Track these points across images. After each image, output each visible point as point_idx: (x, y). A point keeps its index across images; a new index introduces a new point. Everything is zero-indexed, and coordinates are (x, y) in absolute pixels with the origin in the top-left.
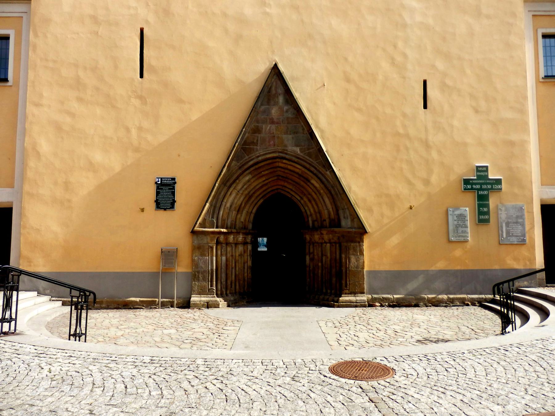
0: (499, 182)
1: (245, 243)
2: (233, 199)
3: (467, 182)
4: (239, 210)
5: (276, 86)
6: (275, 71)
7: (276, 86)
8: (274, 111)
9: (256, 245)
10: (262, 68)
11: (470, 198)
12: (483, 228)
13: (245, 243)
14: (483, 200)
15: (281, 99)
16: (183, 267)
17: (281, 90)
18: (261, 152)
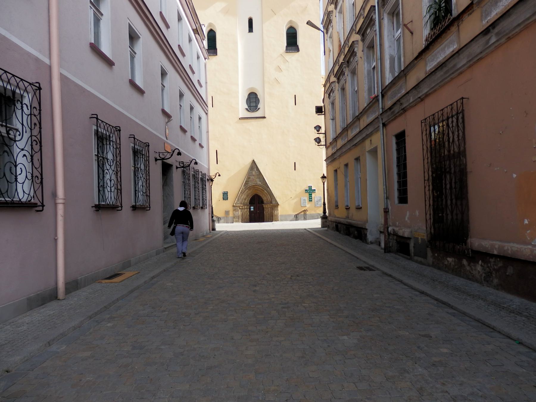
0: (315, 190)
1: (247, 208)
2: (244, 196)
3: (306, 190)
4: (245, 199)
5: (254, 166)
6: (254, 161)
7: (254, 166)
8: (254, 173)
9: (250, 209)
10: (250, 161)
11: (307, 195)
12: (310, 202)
13: (247, 208)
14: (310, 195)
15: (255, 169)
16: (231, 215)
17: (255, 167)
18: (250, 184)
